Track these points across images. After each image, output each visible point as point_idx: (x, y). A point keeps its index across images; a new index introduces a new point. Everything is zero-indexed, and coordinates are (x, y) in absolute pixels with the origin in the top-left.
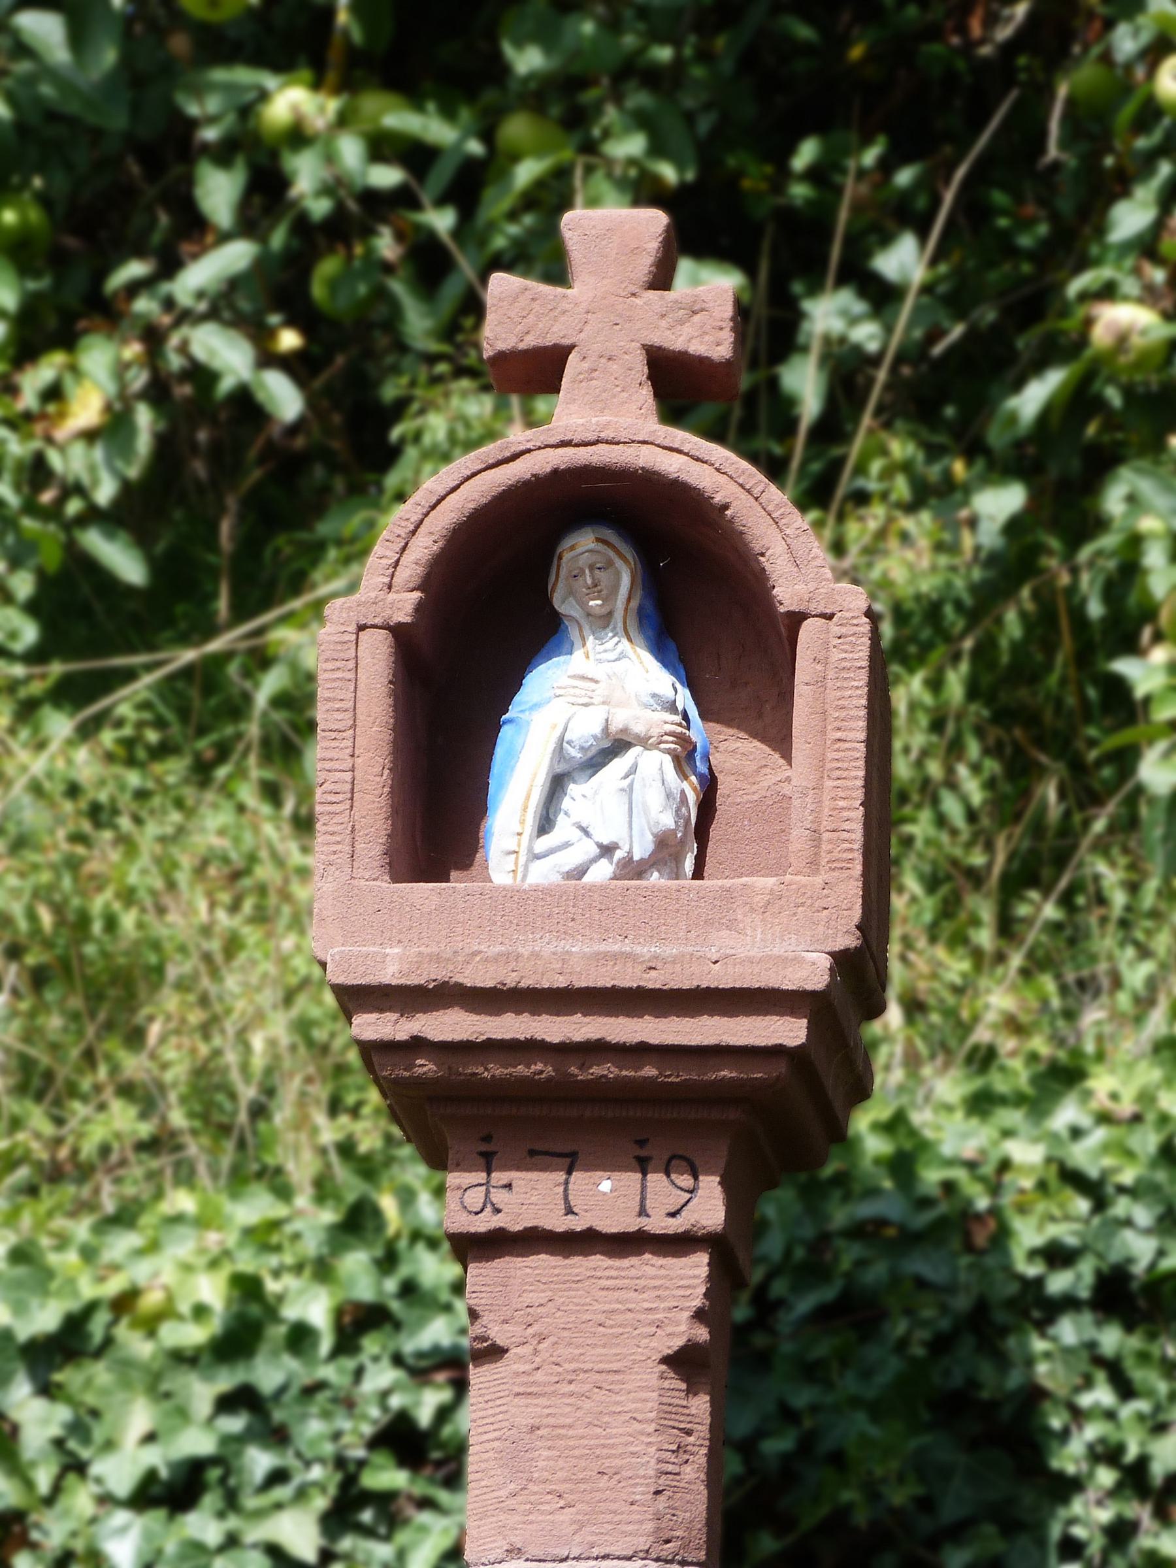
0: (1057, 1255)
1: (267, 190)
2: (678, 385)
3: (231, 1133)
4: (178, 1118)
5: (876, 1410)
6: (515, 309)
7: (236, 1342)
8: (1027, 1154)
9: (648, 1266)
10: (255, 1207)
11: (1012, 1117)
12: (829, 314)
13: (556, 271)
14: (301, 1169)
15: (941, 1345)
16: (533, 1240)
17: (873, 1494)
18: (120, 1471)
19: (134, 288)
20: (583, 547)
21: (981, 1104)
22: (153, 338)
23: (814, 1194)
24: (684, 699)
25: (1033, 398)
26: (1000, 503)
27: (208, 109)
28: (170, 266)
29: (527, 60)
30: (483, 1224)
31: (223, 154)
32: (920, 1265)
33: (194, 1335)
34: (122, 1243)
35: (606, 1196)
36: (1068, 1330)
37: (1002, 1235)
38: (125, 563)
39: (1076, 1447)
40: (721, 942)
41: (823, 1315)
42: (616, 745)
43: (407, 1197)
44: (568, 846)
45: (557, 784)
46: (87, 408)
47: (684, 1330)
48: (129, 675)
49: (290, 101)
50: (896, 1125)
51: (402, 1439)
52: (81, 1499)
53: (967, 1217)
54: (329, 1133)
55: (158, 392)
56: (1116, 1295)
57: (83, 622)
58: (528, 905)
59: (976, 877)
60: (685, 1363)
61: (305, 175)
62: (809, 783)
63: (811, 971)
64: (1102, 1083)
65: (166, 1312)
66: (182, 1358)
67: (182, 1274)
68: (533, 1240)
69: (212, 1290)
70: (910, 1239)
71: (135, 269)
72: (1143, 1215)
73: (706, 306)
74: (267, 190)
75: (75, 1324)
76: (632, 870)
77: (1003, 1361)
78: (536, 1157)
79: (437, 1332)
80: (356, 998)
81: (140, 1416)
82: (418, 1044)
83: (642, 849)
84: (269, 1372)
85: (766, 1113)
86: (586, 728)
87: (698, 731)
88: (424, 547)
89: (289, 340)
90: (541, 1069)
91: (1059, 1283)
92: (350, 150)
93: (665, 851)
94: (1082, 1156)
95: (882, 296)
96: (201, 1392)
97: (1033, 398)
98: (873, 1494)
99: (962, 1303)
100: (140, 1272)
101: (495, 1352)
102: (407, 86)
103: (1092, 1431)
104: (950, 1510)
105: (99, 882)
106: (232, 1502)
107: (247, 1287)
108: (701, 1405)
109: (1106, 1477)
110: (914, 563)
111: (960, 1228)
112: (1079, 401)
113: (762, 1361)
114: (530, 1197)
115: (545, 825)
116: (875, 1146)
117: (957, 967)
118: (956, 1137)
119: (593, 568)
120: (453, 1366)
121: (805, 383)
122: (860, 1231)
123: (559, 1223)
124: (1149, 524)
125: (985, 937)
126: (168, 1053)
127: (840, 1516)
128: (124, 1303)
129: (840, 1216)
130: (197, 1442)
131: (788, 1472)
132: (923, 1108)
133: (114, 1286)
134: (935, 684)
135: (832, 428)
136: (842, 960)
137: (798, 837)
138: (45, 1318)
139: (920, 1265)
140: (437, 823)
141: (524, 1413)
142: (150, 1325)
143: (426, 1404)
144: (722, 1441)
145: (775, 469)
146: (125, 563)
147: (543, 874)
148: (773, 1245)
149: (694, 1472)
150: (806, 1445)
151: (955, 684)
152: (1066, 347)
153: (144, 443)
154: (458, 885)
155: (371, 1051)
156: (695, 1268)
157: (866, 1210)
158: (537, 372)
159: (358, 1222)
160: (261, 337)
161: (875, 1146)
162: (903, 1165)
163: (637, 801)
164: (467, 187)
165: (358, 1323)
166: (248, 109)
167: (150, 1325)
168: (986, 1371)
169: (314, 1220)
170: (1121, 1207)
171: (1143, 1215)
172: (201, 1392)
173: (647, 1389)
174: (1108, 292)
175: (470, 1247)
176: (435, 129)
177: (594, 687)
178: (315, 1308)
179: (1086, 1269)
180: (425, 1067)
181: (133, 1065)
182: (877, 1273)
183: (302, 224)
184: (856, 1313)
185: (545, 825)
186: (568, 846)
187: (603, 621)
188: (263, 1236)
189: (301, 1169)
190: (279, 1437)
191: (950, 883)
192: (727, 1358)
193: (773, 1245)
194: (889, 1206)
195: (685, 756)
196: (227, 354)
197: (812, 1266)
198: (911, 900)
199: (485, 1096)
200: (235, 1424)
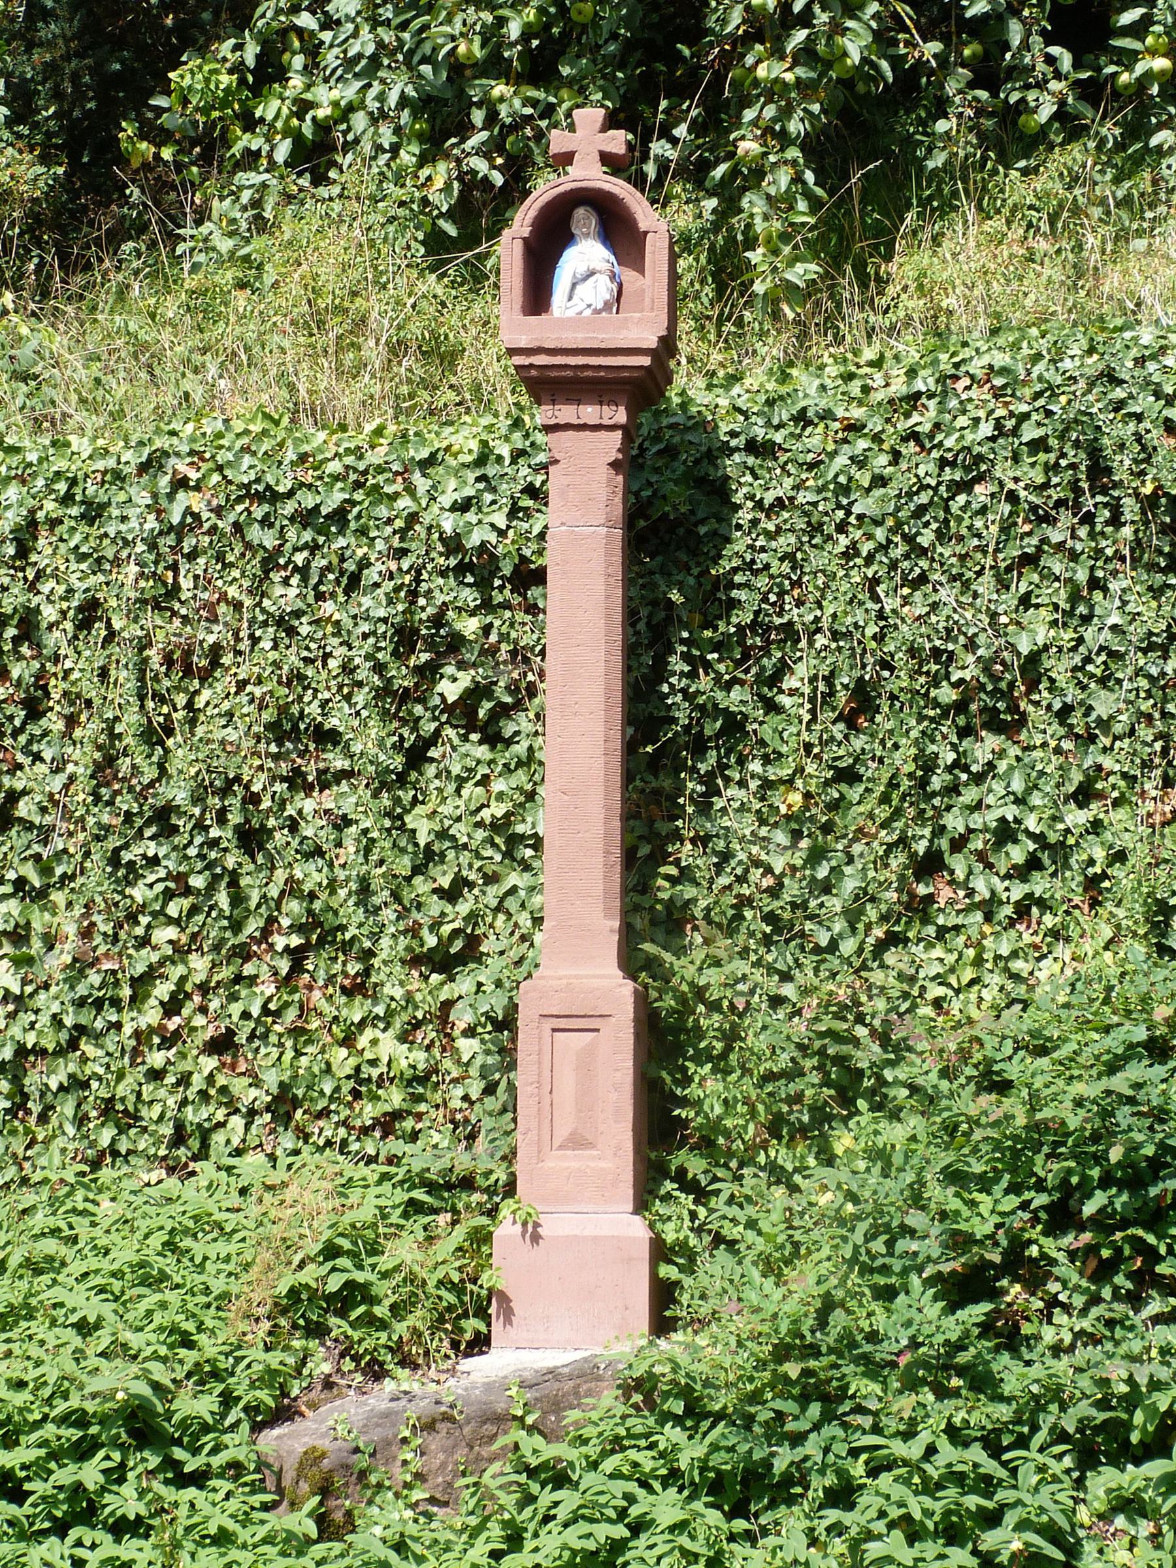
0: (733, 434)
1: (492, 118)
2: (606, 159)
3: (480, 399)
4: (468, 396)
5: (676, 482)
6: (558, 140)
7: (481, 461)
8: (724, 402)
9: (603, 434)
10: (487, 420)
11: (720, 391)
12: (658, 147)
13: (572, 128)
14: (503, 410)
15: (697, 462)
16: (568, 427)
17: (675, 508)
18: (446, 500)
19: (453, 145)
20: (580, 212)
21: (710, 387)
22: (459, 161)
23: (658, 414)
24: (612, 258)
25: (719, 171)
26: (711, 203)
27: (475, 94)
28: (463, 141)
29: (565, 71)
30: (552, 422)
31: (479, 105)
32: (689, 437)
33: (469, 459)
34: (448, 430)
35: (590, 413)
36: (737, 458)
37: (717, 426)
38: (451, 230)
39: (740, 494)
40: (624, 334)
41: (660, 453)
42: (592, 273)
43: (532, 416)
44: (578, 304)
45: (574, 285)
46: (439, 183)
47: (614, 455)
48: (451, 260)
49: (500, 89)
50: (683, 393)
51: (531, 491)
52: (435, 509)
53: (705, 422)
54: (511, 399)
55: (460, 178)
56: (752, 447)
57: (436, 243)
58: (564, 323)
59: (708, 318)
60: (615, 465)
61: (503, 110)
62: (651, 282)
63: (652, 342)
64: (747, 381)
65: (460, 452)
66: (464, 465)
67: (464, 440)
68: (568, 427)
69: (474, 445)
70: (688, 429)
71: (453, 140)
72: (760, 422)
73: (618, 141)
74: (492, 118)
75: (433, 455)
76: (597, 312)
77: (717, 467)
78: (568, 401)
79: (542, 458)
80: (512, 352)
81: (453, 483)
82: (531, 366)
83: (600, 305)
84: (491, 470)
85: (640, 387)
86: (582, 270)
87: (617, 269)
88: (532, 213)
89: (499, 161)
90: (569, 373)
91: (734, 443)
92: (517, 103)
93: (607, 306)
94: (740, 403)
95: (674, 141)
96: (471, 476)
97: (719, 171)
98: (675, 508)
99: (704, 449)
100: (453, 439)
101: (557, 462)
102: (535, 83)
103: (745, 490)
104: (700, 515)
105: (443, 324)
106: (480, 509)
107: (484, 443)
108: (620, 478)
109: (750, 504)
110: (685, 219)
111: (702, 425)
112: (734, 172)
113: (642, 467)
114: (566, 413)
115: (570, 298)
116: (676, 400)
117: (704, 346)
118: (701, 397)
119: (584, 219)
120: (544, 467)
121: (650, 169)
122: (672, 426)
123: (576, 422)
124: (755, 210)
125: (712, 337)
126: (463, 375)
127: (665, 515)
128: (448, 449)
129: (665, 422)
130: (469, 492)
131: (650, 501)
132: (688, 387)
133: (444, 445)
134: (697, 260)
135: (659, 181)
136: (662, 339)
137: (647, 300)
138: (424, 454)
139: (689, 437)
140: (537, 297)
141: (566, 481)
142: (455, 455)
143: (538, 480)
144: (627, 491)
145: (643, 191)
146: (451, 230)
147: (571, 313)
148: (644, 431)
149: (618, 499)
150: (655, 493)
151: (703, 260)
152: (731, 155)
153: (456, 193)
154: (544, 317)
155: (517, 367)
156: (618, 434)
157: (673, 420)
158: (567, 158)
159: (517, 424)
160: (491, 160)
161: (676, 400)
162: (684, 406)
163: (599, 290)
164: (549, 111)
165: (518, 455)
166: (486, 93)
167: (455, 455)
168: (711, 470)
169: (504, 424)
170: (753, 419)
171: (760, 422)
172: (471, 476)
173: (603, 473)
174: (743, 138)
175: (548, 429)
176: (540, 94)
177: (586, 255)
178: (505, 451)
179: (743, 438)
180: (534, 373)
181: (453, 380)
182: (677, 439)
183: (503, 126)
184: (670, 452)
185: (570, 298)
186: (578, 304)
187: (587, 235)
188: (489, 428)
189: (503, 410)
190: (494, 490)
191: (700, 319)
192: (630, 464)
193: (644, 431)
194: (680, 419)
195: (613, 277)
196: (480, 165)
197: (657, 439)
198: (685, 326)
199: (552, 382)
200: (482, 486)
